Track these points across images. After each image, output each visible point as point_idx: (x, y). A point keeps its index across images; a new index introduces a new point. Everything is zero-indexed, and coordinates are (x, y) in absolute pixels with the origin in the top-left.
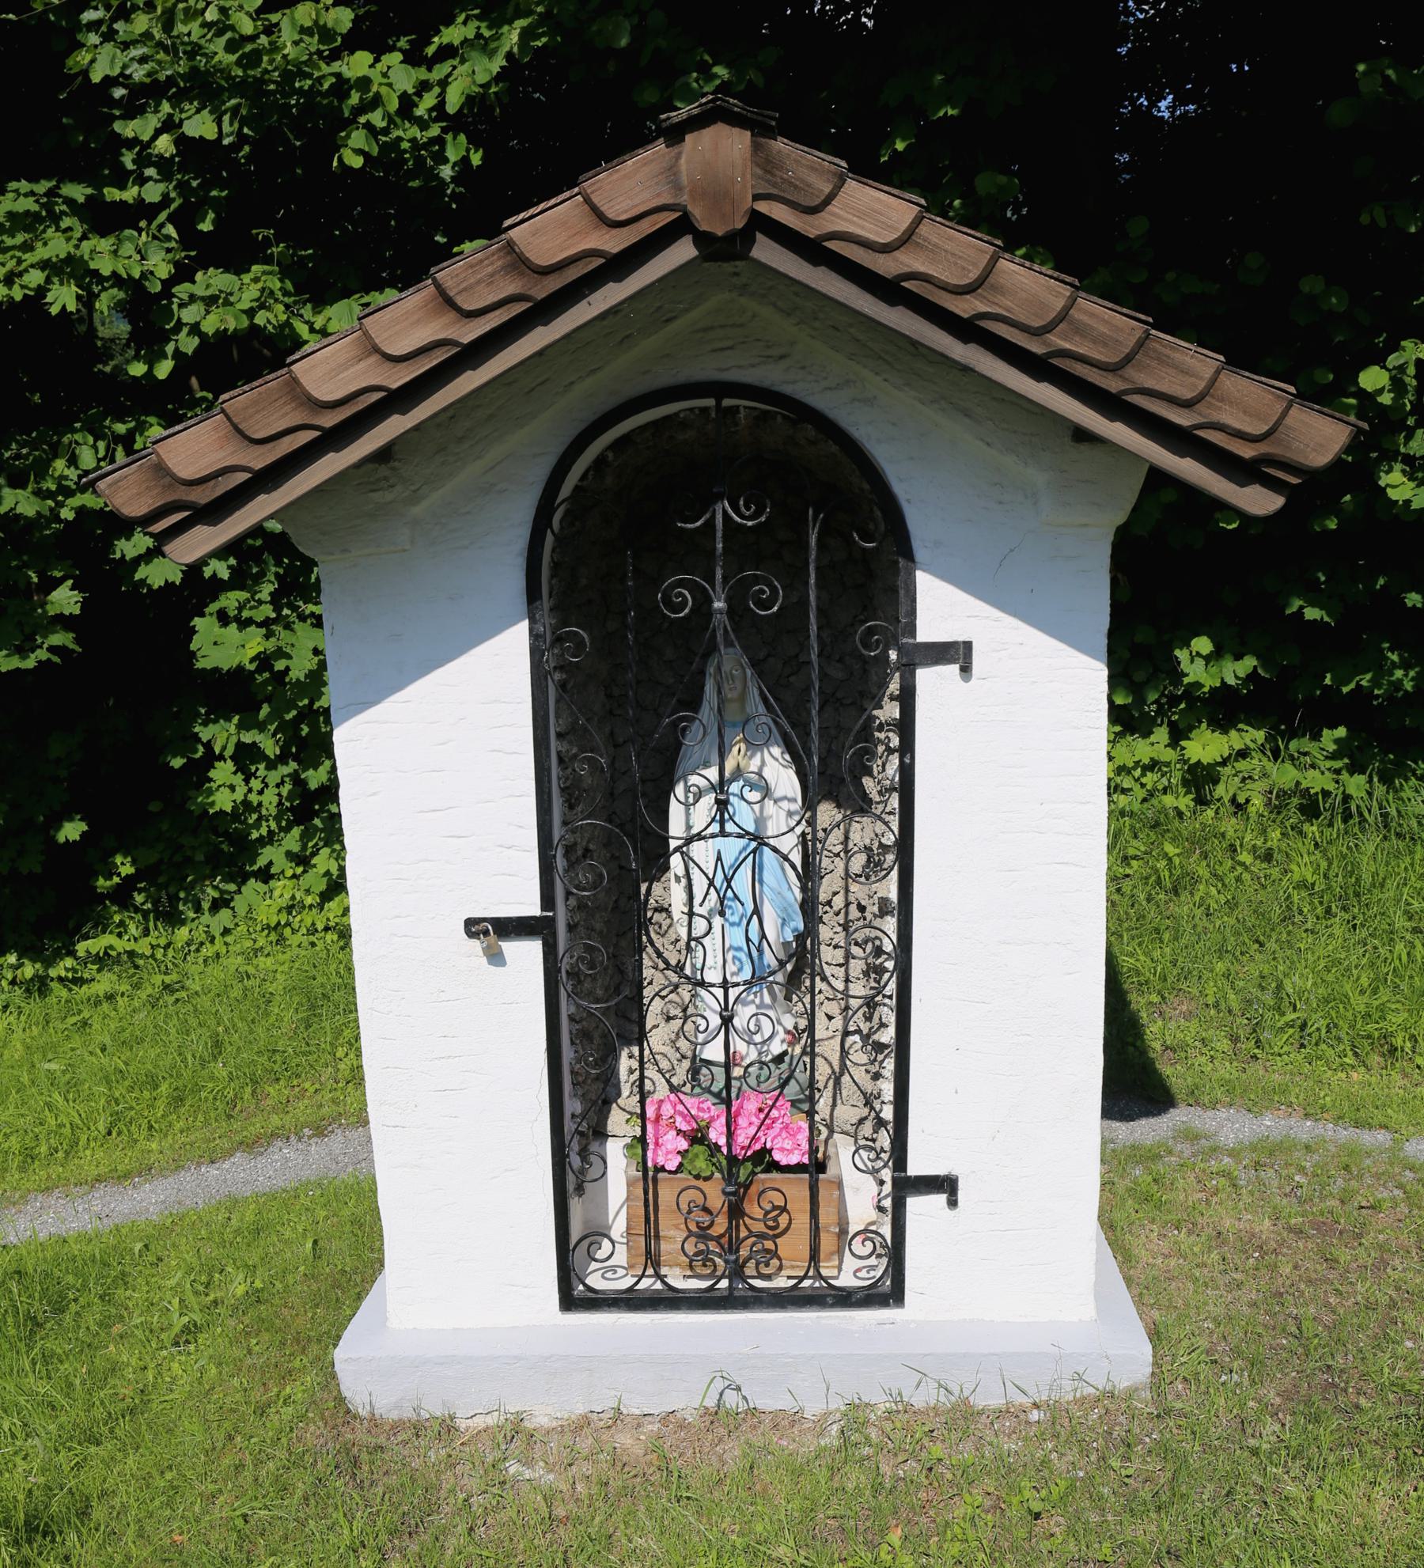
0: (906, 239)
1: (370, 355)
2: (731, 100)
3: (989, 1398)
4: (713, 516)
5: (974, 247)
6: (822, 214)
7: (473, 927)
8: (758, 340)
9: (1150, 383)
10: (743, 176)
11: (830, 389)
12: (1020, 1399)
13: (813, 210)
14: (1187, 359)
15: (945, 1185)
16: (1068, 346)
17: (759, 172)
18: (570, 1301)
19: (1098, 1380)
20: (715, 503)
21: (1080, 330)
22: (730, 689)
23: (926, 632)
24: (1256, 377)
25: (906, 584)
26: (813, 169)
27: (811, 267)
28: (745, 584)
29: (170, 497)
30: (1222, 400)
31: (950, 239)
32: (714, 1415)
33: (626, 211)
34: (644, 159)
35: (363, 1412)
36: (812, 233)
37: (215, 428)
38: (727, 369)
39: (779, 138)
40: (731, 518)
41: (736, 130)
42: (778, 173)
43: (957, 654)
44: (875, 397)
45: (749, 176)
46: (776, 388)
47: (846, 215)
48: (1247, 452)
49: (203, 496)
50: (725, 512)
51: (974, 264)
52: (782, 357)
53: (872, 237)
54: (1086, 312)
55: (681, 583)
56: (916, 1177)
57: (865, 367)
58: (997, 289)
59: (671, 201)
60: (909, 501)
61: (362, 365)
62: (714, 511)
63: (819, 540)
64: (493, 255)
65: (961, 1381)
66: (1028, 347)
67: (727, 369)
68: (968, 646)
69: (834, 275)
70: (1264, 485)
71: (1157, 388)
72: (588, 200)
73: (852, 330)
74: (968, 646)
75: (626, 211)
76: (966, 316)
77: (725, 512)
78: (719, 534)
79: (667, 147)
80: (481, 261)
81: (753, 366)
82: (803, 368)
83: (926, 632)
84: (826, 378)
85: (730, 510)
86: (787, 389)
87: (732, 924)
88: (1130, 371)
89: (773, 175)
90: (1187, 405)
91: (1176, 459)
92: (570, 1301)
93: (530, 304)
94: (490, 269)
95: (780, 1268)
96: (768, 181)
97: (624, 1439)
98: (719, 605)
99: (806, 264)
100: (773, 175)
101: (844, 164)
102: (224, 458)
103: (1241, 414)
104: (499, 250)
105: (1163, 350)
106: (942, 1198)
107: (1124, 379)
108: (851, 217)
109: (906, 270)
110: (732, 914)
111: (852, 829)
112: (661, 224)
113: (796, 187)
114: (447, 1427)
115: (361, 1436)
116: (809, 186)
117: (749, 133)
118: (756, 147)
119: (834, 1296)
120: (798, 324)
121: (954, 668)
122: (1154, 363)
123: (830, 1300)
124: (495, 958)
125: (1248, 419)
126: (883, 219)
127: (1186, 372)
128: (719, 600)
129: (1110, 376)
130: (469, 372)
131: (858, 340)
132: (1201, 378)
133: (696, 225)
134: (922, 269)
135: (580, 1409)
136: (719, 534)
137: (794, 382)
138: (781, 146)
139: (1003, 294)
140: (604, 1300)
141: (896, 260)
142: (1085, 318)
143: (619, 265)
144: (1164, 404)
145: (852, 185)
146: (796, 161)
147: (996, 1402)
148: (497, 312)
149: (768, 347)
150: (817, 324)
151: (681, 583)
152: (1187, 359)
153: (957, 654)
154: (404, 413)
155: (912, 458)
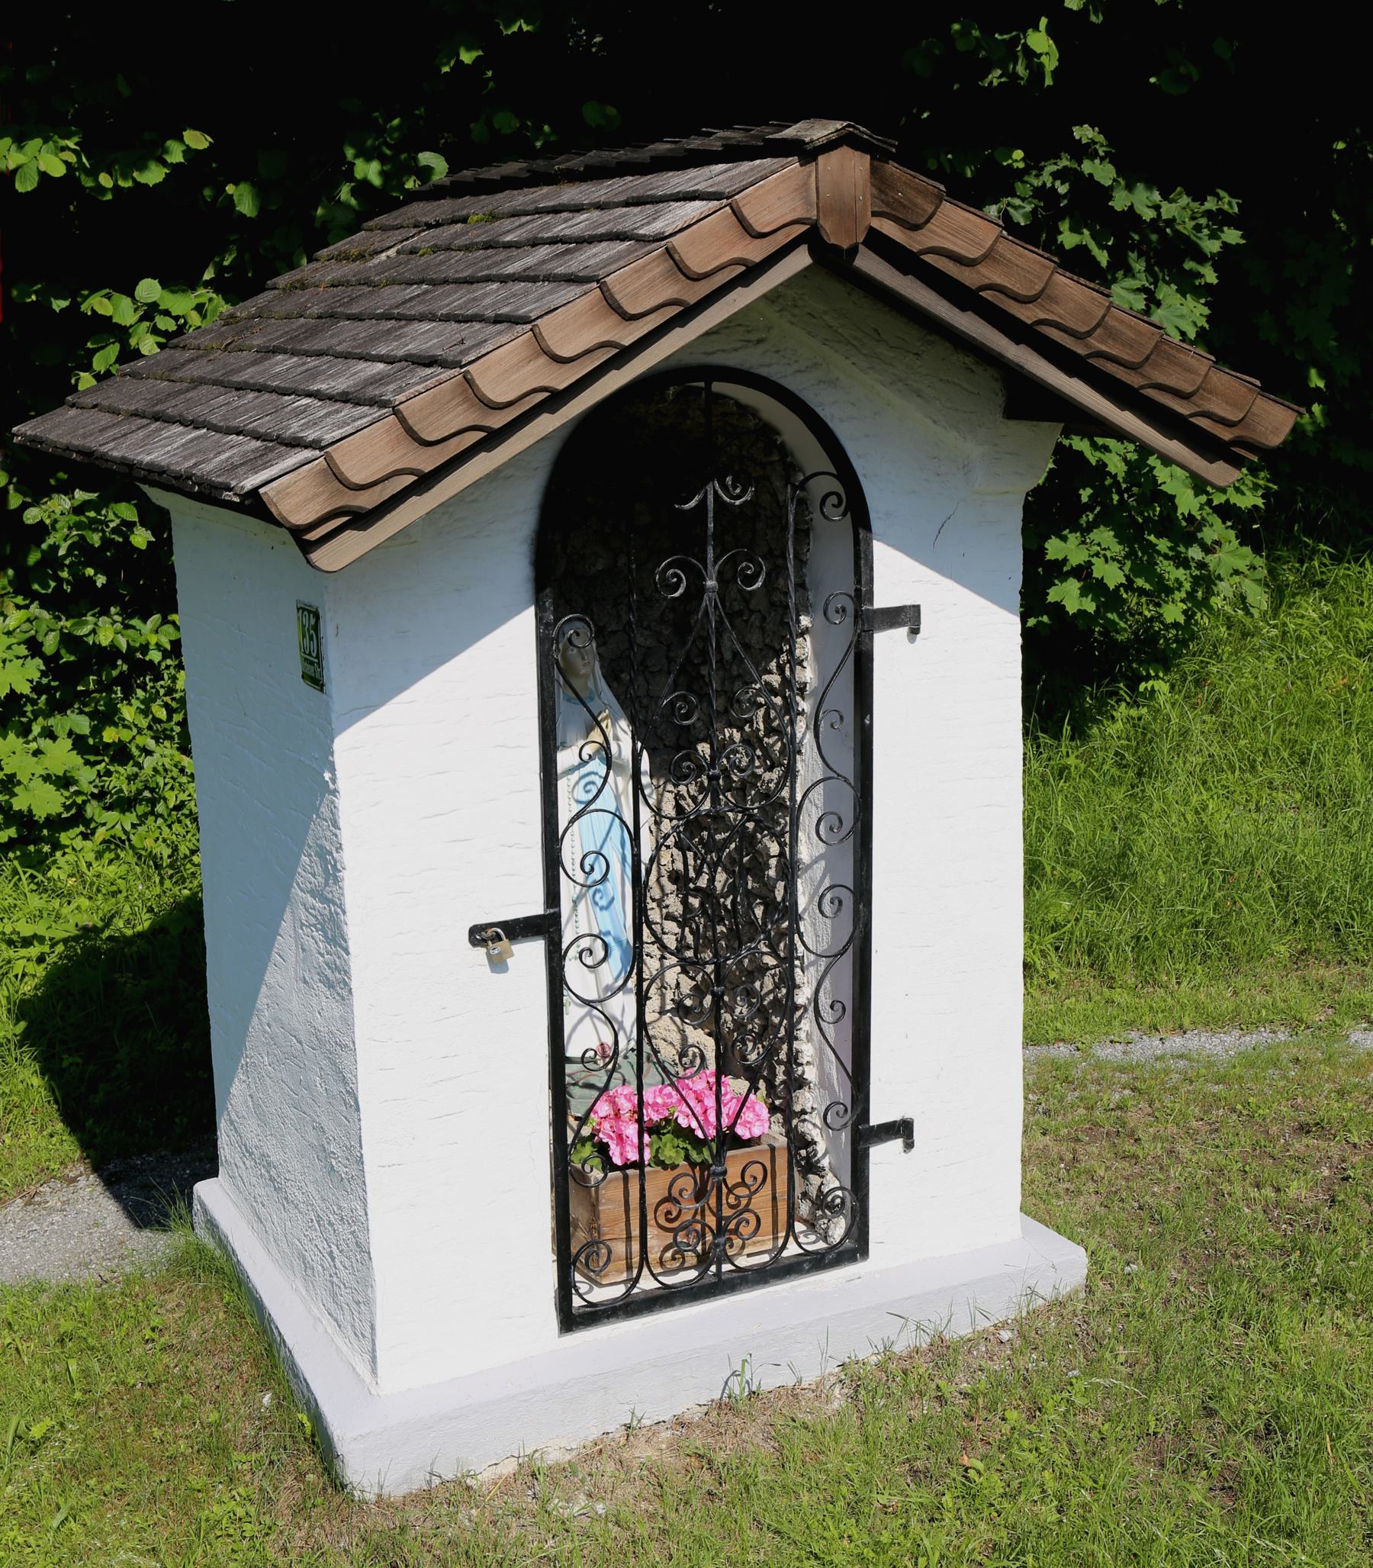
0: (988, 256)
1: (538, 356)
2: (861, 128)
3: (961, 1328)
4: (705, 498)
5: (1039, 262)
6: (923, 231)
7: (479, 935)
8: (740, 325)
9: (1161, 379)
10: (864, 195)
11: (800, 371)
12: (983, 1324)
13: (915, 228)
14: (1189, 359)
15: (902, 1130)
16: (1103, 348)
17: (875, 192)
18: (570, 1320)
19: (1046, 1291)
20: (707, 483)
21: (1112, 335)
22: (584, 665)
23: (883, 598)
24: (1234, 373)
25: (866, 555)
26: (919, 192)
27: (902, 276)
28: (733, 561)
29: (339, 503)
30: (1211, 392)
31: (1020, 255)
32: (726, 1406)
33: (768, 224)
34: (782, 176)
35: (371, 1497)
36: (915, 247)
37: (387, 431)
38: (713, 353)
39: (891, 162)
40: (721, 497)
41: (858, 154)
42: (891, 194)
43: (907, 617)
44: (838, 379)
45: (869, 196)
46: (756, 371)
47: (945, 234)
48: (1226, 435)
49: (367, 501)
50: (715, 492)
51: (1039, 278)
52: (760, 341)
53: (963, 252)
54: (1117, 319)
55: (669, 566)
56: (878, 1126)
57: (837, 351)
58: (1053, 299)
59: (804, 216)
60: (865, 476)
61: (532, 366)
62: (706, 491)
63: (794, 519)
64: (654, 260)
65: (934, 1317)
66: (1074, 348)
67: (713, 353)
68: (916, 609)
69: (919, 282)
70: (1227, 461)
71: (1167, 383)
72: (736, 213)
73: (826, 317)
74: (916, 609)
75: (768, 224)
76: (1029, 322)
77: (715, 492)
78: (711, 515)
79: (801, 165)
80: (644, 267)
81: (736, 350)
82: (777, 352)
83: (883, 598)
84: (796, 362)
85: (720, 492)
86: (764, 372)
87: (602, 908)
88: (1147, 369)
89: (886, 195)
90: (1185, 396)
91: (1166, 441)
92: (570, 1320)
93: (681, 308)
94: (650, 275)
95: (743, 1247)
96: (882, 201)
97: (643, 1452)
98: (711, 583)
99: (897, 273)
100: (886, 195)
101: (942, 188)
102: (396, 460)
103: (1224, 405)
104: (659, 256)
105: (1171, 351)
106: (898, 1143)
107: (1143, 376)
108: (945, 234)
109: (987, 281)
110: (601, 898)
111: (665, 799)
112: (794, 236)
113: (905, 207)
114: (460, 1491)
115: (382, 1524)
116: (916, 205)
117: (868, 157)
118: (874, 170)
119: (810, 1261)
120: (781, 311)
121: (903, 631)
122: (1165, 362)
123: (806, 1266)
124: (498, 964)
125: (1229, 408)
126: (972, 237)
127: (1188, 370)
128: (711, 579)
129: (1132, 373)
130: (614, 372)
131: (831, 327)
132: (1199, 375)
133: (825, 238)
134: (999, 281)
135: (595, 1434)
136: (711, 515)
137: (769, 365)
138: (892, 168)
139: (1057, 303)
140: (604, 1311)
141: (979, 273)
142: (1115, 323)
143: (752, 272)
144: (1169, 396)
145: (946, 206)
146: (905, 183)
147: (966, 1331)
148: (653, 316)
149: (749, 332)
150: (796, 311)
151: (669, 566)
152: (1189, 359)
153: (907, 617)
154: (553, 412)
155: (867, 436)
